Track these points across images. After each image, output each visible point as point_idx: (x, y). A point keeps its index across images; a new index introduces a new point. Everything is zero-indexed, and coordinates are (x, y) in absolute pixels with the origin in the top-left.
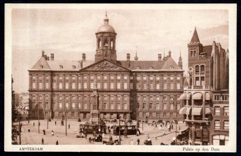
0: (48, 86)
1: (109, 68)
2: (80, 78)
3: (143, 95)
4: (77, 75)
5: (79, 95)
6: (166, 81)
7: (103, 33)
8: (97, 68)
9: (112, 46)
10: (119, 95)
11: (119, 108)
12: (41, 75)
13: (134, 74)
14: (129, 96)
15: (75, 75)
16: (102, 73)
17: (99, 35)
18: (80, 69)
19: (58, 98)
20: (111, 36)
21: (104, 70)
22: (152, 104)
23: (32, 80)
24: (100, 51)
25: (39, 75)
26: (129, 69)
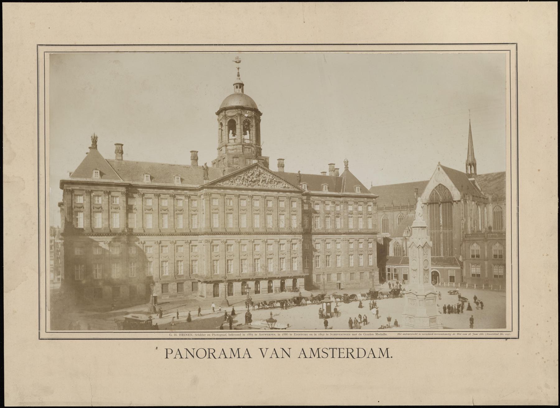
1: (265, 185)
15: (183, 198)
16: (250, 193)
21: (256, 187)
24: (235, 147)
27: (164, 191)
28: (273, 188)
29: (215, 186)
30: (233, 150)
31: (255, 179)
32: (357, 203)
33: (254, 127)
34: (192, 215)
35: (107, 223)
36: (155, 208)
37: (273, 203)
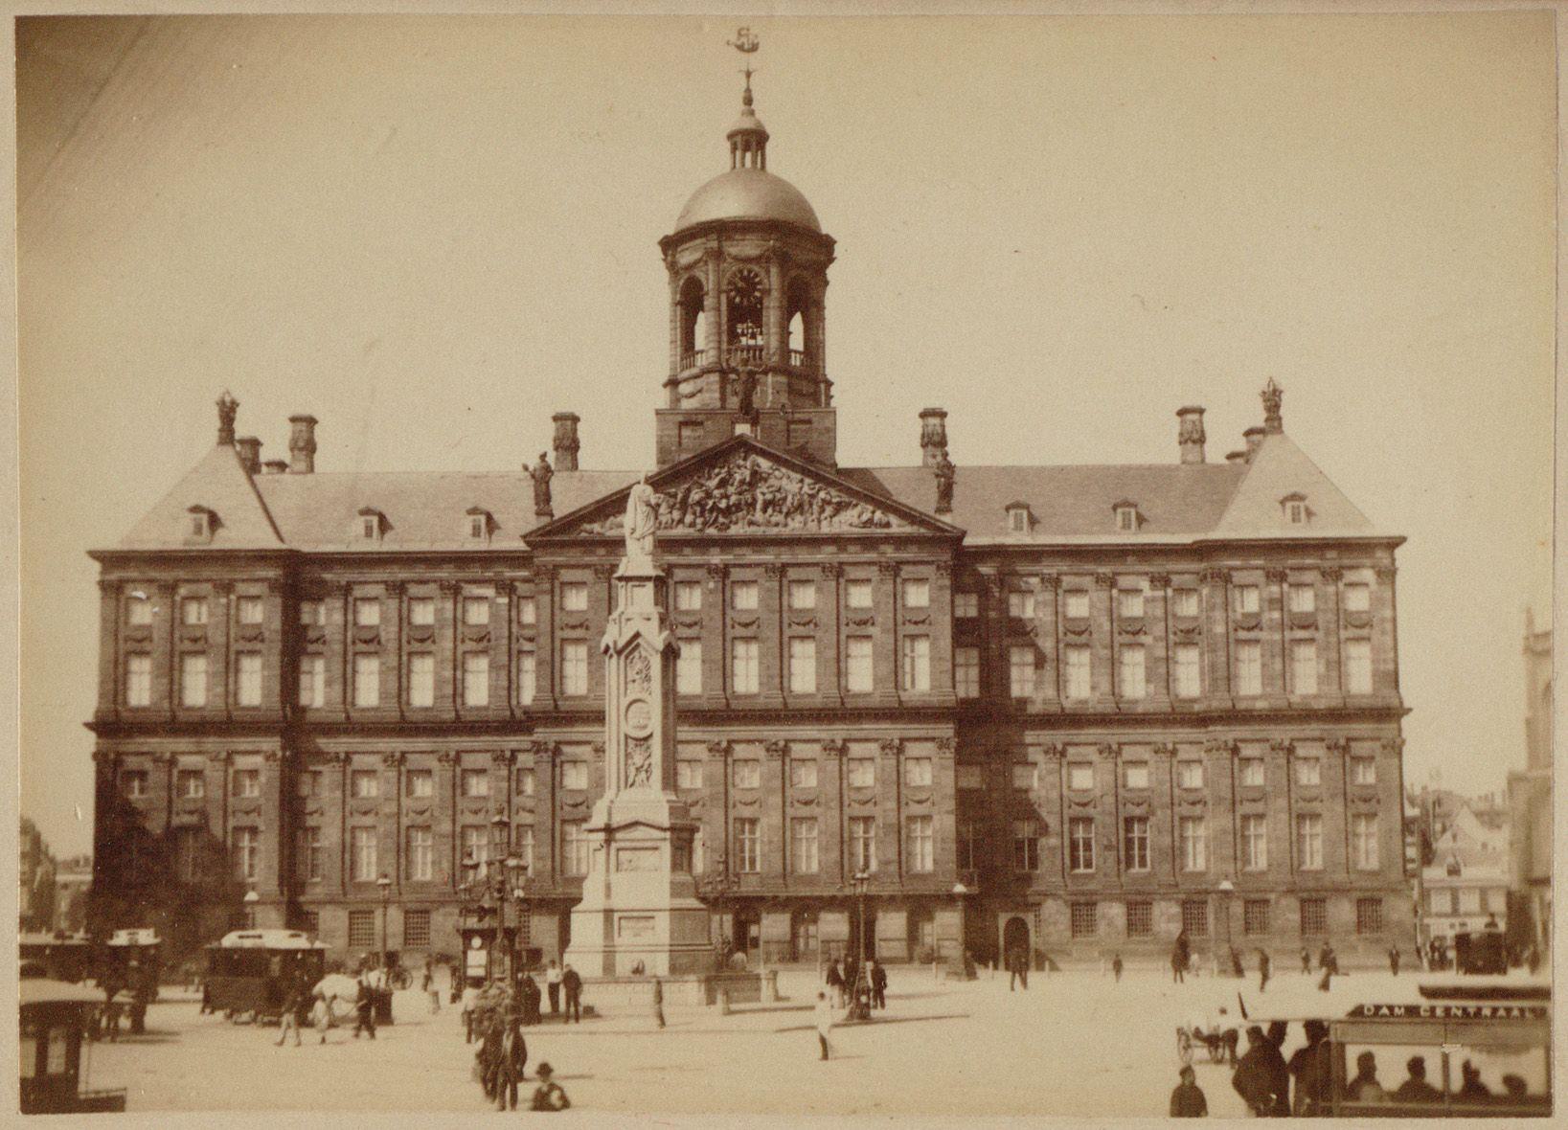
0: (254, 686)
1: (779, 518)
2: (529, 614)
3: (1071, 750)
4: (507, 588)
5: (525, 760)
6: (1253, 623)
7: (723, 229)
8: (676, 515)
9: (797, 342)
10: (867, 745)
11: (874, 855)
12: (206, 588)
13: (986, 569)
14: (950, 754)
15: (489, 592)
16: (716, 558)
17: (686, 257)
18: (533, 523)
19: (348, 788)
20: (784, 260)
21: (735, 531)
22: (1143, 820)
23: (126, 639)
24: (700, 383)
25: (183, 591)
26: (947, 518)
27: (476, 572)
28: (812, 528)
29: (573, 537)
30: (692, 395)
31: (733, 499)
32: (1281, 577)
33: (775, 294)
34: (520, 652)
35: (220, 690)
36: (389, 634)
37: (819, 590)
